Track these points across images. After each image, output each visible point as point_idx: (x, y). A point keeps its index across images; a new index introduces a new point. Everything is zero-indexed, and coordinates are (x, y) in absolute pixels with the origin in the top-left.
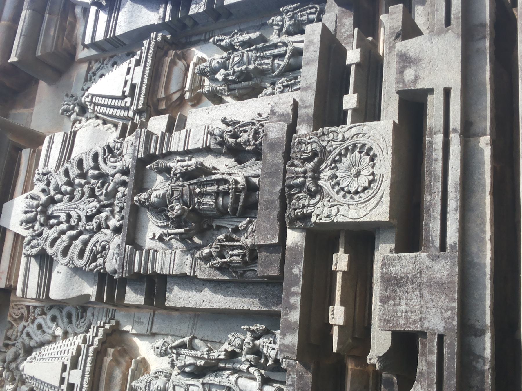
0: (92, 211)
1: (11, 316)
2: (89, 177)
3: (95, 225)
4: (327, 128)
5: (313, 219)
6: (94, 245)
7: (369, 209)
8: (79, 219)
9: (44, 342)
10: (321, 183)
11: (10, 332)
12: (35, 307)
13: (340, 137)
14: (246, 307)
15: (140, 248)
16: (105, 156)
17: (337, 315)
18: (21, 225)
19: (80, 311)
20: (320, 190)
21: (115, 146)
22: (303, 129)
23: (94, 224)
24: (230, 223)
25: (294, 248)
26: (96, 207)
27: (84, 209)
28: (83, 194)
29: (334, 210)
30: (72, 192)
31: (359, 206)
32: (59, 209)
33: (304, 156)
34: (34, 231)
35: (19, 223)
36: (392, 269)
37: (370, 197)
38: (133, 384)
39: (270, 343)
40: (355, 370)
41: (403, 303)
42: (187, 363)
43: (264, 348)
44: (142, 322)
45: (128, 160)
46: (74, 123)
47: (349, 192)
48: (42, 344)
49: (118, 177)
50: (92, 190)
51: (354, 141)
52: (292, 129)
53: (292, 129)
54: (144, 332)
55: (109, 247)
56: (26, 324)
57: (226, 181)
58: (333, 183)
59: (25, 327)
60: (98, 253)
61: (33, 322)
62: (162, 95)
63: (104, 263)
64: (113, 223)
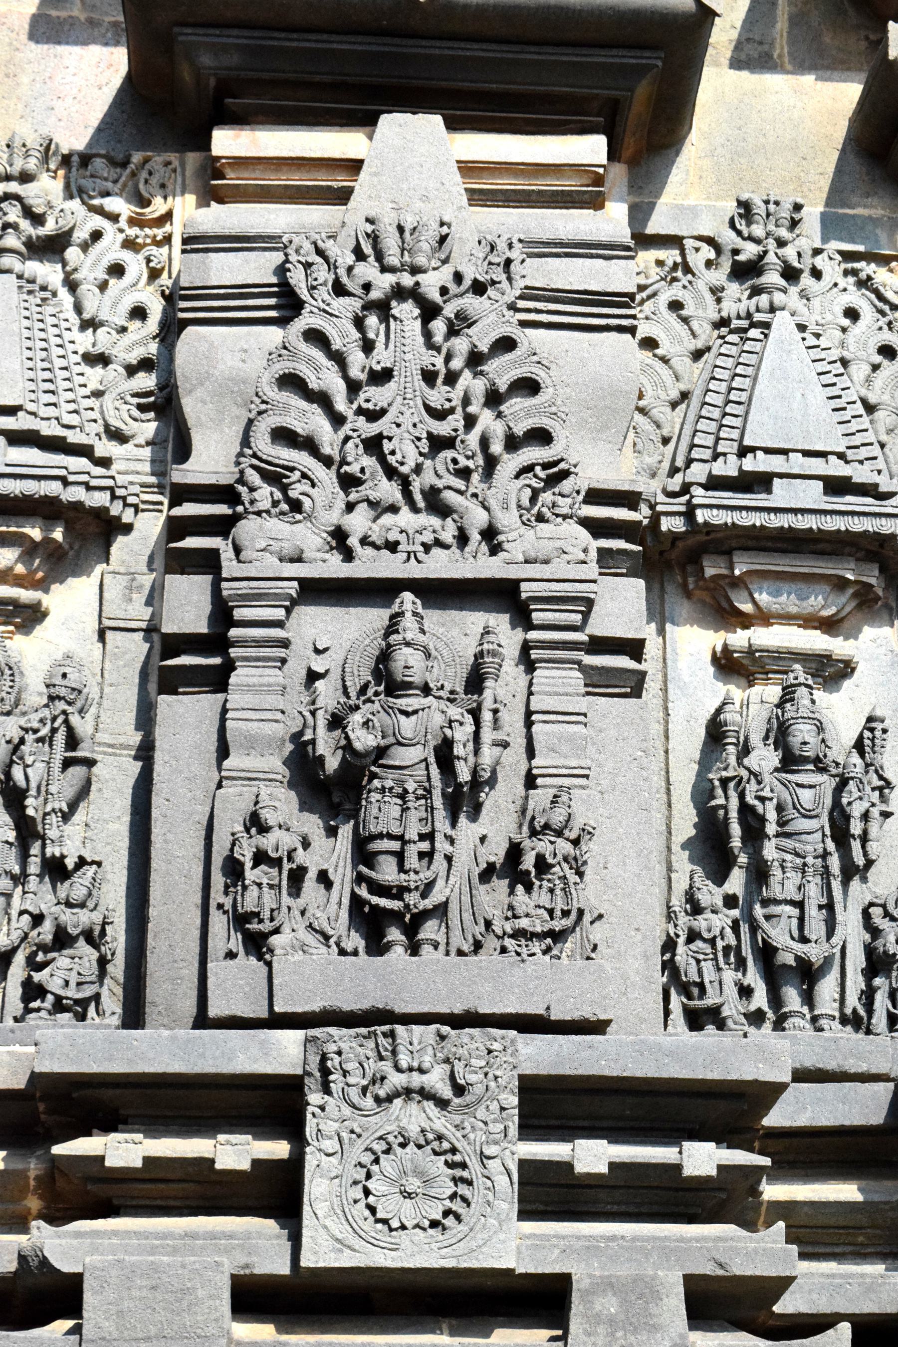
0: (393, 453)
1: (146, 160)
3: (353, 469)
4: (516, 1119)
6: (304, 476)
7: (328, 1222)
8: (374, 416)
9: (78, 291)
11: (99, 164)
14: (155, 914)
16: (538, 469)
17: (123, 1150)
18: (368, 220)
21: (563, 496)
24: (341, 864)
25: (265, 1049)
26: (402, 464)
27: (398, 425)
28: (440, 415)
29: (331, 1145)
31: (336, 1201)
32: (405, 341)
34: (350, 269)
35: (372, 214)
37: (354, 1225)
39: (79, 974)
40: (28, 1177)
42: (29, 770)
43: (68, 960)
44: (131, 600)
46: (710, 241)
47: (369, 1176)
48: (72, 286)
49: (477, 518)
50: (448, 443)
51: (480, 1182)
54: (107, 611)
55: (299, 522)
56: (123, 223)
57: (427, 856)
58: (391, 1138)
59: (114, 218)
60: (284, 489)
61: (130, 244)
63: (258, 513)
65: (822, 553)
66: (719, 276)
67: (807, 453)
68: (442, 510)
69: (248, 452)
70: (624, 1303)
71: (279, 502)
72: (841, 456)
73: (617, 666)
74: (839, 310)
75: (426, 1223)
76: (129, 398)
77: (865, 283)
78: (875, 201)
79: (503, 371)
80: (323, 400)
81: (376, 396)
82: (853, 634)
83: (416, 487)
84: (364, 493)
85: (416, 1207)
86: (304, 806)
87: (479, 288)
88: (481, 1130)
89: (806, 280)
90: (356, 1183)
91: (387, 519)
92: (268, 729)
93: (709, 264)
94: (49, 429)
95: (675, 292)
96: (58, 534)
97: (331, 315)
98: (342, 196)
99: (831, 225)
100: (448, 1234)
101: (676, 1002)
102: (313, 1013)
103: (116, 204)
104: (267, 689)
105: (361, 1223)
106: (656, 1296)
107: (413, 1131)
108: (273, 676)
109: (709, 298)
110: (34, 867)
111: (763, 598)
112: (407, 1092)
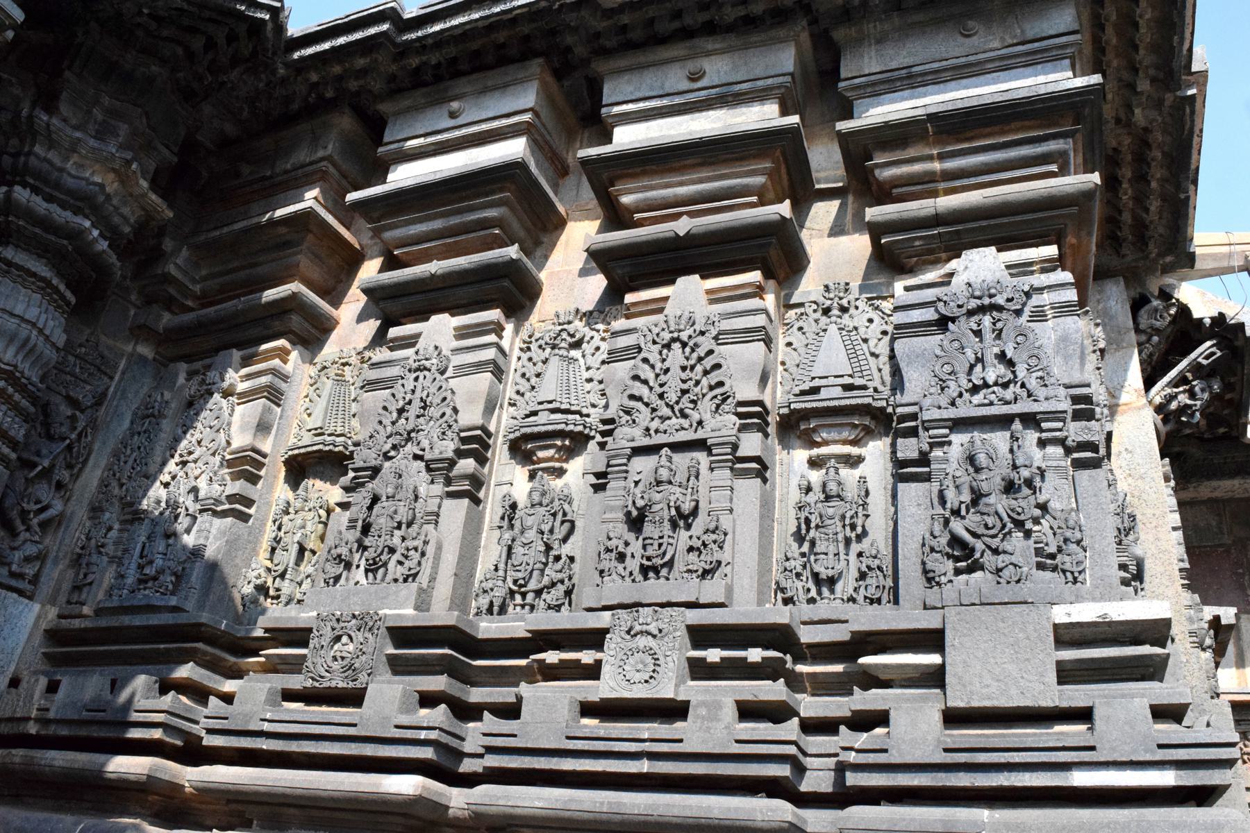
23: (657, 403)
59: (598, 331)
65: (847, 415)
66: (818, 315)
67: (836, 377)
68: (685, 416)
70: (709, 711)
72: (850, 376)
73: (761, 468)
74: (865, 320)
77: (877, 308)
79: (708, 363)
80: (645, 382)
81: (663, 378)
82: (865, 445)
83: (677, 408)
86: (630, 530)
89: (852, 311)
91: (668, 422)
92: (618, 503)
93: (815, 311)
94: (563, 407)
95: (801, 323)
96: (567, 443)
98: (661, 310)
99: (862, 289)
101: (780, 595)
103: (601, 327)
104: (619, 488)
106: (721, 708)
107: (641, 647)
108: (622, 483)
111: (824, 435)
112: (642, 632)
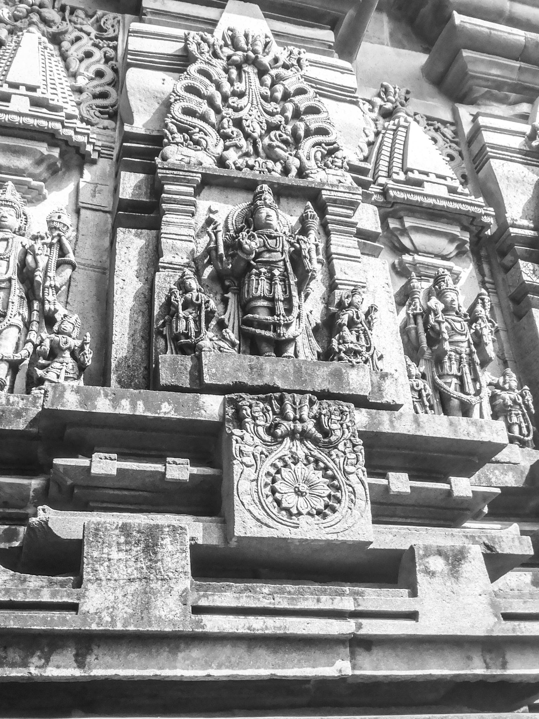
0: (248, 126)
1: (104, 15)
2: (295, 124)
3: (229, 131)
4: (363, 451)
5: (237, 432)
6: (201, 130)
7: (251, 508)
8: (237, 110)
9: (68, 60)
10: (287, 440)
11: (81, 13)
12: (115, 48)
13: (350, 469)
14: (116, 339)
15: (198, 192)
16: (323, 145)
17: (104, 465)
18: (229, 29)
19: (110, 110)
20: (277, 440)
21: (338, 158)
22: (361, 418)
23: (230, 129)
24: (232, 317)
26: (253, 132)
27: (250, 115)
28: (272, 114)
30: (275, 100)
31: (255, 496)
33: (325, 419)
34: (221, 48)
35: (232, 27)
36: (167, 540)
37: (268, 510)
38: (10, 183)
39: (66, 372)
40: (29, 489)
41: (122, 555)
42: (38, 257)
44: (95, 196)
45: (318, 176)
46: (369, 102)
47: (274, 481)
48: (64, 57)
49: (294, 163)
50: (277, 127)
51: (345, 488)
52: (361, 402)
53: (361, 402)
54: (81, 199)
55: (198, 150)
56: (92, 36)
57: (289, 311)
58: (287, 458)
59: (89, 34)
60: (190, 135)
61: (95, 45)
62: (409, 222)
63: (177, 144)
64: (232, 156)
69: (170, 115)
71: (187, 140)
75: (315, 512)
76: (94, 107)
78: (436, 100)
84: (234, 142)
85: (306, 500)
87: (286, 67)
88: (342, 456)
90: (266, 485)
97: (211, 65)
100: (328, 519)
102: (228, 385)
105: (272, 510)
109: (372, 123)
110: (35, 316)
